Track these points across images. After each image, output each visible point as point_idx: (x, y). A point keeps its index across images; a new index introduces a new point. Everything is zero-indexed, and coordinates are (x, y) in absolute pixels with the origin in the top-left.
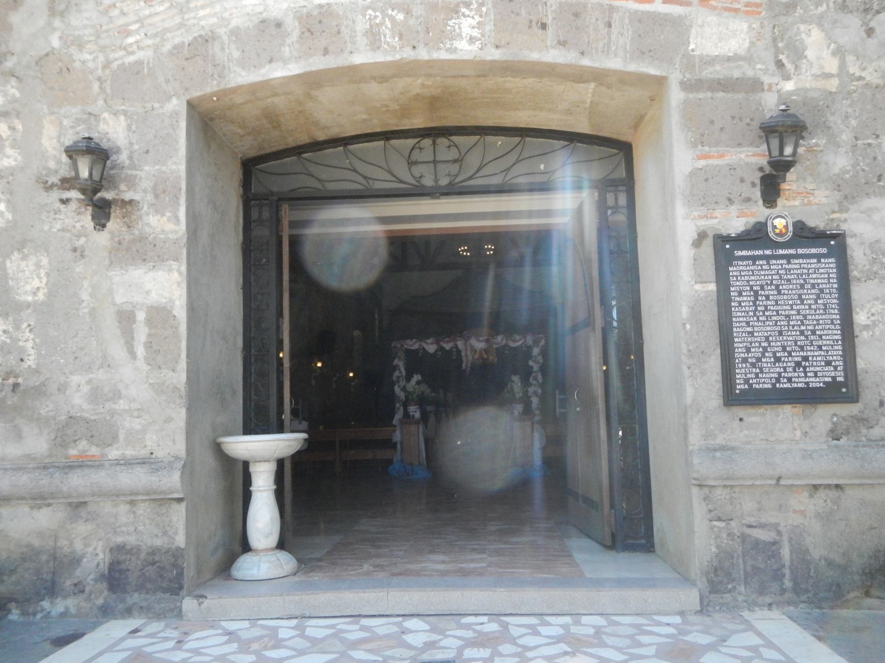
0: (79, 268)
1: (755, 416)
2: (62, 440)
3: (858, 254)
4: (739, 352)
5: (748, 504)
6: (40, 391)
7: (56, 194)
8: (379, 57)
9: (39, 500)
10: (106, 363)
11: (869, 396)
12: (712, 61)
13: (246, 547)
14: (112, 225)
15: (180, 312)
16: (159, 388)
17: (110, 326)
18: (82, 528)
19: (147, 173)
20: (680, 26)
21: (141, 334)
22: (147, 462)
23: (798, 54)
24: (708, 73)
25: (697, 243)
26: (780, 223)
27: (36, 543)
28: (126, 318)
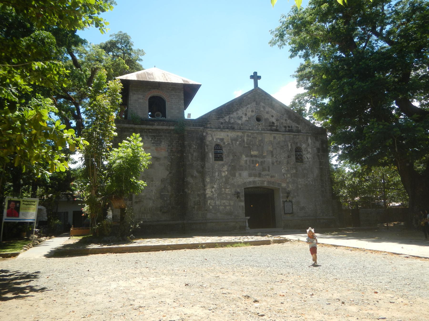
3: (293, 203)
8: (259, 185)
14: (238, 199)
15: (244, 206)
19: (241, 194)
20: (281, 184)
22: (242, 219)
23: (289, 187)
28: (240, 207)
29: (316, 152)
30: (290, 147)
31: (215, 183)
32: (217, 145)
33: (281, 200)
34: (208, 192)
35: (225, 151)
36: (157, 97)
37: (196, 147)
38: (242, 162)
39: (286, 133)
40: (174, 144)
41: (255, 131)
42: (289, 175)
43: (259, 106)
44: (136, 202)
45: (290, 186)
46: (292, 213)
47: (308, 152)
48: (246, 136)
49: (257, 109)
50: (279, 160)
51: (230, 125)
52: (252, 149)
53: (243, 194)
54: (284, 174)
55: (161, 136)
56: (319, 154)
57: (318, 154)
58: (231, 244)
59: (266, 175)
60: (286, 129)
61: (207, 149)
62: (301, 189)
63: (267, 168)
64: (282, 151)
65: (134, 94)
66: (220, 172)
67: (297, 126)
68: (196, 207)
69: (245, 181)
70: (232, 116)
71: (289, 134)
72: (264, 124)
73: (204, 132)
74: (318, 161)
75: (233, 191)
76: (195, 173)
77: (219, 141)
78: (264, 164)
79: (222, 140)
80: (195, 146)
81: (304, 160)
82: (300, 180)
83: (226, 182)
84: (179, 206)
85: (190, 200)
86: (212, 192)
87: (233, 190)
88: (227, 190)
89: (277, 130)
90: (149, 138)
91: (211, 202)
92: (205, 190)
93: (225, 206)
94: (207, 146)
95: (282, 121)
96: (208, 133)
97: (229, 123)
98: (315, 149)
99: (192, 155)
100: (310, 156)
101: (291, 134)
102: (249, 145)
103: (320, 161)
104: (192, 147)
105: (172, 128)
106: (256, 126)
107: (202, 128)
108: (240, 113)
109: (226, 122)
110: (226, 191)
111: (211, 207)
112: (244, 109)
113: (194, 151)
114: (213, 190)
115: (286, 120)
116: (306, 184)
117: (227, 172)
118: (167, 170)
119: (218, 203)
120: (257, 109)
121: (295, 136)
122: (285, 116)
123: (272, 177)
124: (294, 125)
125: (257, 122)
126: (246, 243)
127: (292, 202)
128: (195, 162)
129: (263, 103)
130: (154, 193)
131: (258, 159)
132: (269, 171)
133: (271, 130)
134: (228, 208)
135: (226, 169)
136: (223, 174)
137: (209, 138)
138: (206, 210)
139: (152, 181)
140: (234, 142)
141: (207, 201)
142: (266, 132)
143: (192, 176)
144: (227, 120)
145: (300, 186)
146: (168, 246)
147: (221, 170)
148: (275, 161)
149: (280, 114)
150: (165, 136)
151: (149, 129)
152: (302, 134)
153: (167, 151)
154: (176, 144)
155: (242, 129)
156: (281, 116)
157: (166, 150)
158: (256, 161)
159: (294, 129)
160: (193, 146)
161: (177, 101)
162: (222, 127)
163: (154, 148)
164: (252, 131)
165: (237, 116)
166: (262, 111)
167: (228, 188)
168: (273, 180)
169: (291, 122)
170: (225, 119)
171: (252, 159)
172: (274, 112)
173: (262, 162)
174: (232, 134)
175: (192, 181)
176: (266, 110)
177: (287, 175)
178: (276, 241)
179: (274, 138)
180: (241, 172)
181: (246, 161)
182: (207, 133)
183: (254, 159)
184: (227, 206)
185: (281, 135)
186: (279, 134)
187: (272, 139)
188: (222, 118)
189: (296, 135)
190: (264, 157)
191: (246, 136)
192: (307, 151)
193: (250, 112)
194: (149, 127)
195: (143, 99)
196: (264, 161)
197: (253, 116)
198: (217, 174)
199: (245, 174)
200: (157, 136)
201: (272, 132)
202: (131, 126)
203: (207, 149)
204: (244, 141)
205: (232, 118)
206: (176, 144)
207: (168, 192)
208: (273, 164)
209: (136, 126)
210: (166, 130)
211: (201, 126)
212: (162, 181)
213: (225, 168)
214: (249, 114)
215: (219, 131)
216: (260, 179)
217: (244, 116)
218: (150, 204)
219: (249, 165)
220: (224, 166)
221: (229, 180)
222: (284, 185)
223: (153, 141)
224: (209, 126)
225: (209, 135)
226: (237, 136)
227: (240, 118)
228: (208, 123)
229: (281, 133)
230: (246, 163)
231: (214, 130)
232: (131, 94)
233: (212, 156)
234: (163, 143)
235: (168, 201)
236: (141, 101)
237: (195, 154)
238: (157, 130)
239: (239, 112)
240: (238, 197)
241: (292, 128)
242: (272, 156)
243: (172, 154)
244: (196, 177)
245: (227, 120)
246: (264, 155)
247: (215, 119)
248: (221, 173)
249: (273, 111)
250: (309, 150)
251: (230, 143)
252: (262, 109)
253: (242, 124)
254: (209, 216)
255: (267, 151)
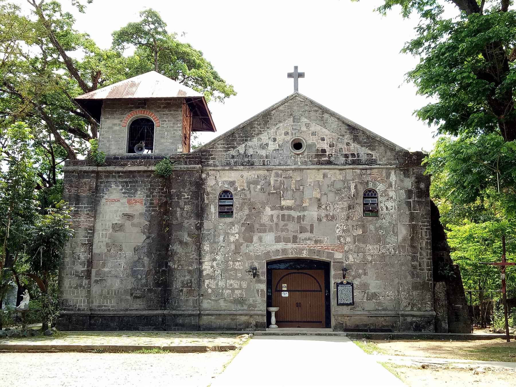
0: (251, 283)
1: (341, 307)
2: (249, 307)
3: (355, 286)
4: (339, 299)
5: (340, 318)
6: (246, 300)
7: (248, 273)
9: (246, 315)
10: (255, 297)
11: (355, 304)
12: (337, 259)
13: (271, 324)
16: (262, 301)
17: (255, 292)
18: (252, 319)
19: (260, 271)
20: (333, 254)
21: (260, 293)
24: (338, 260)
25: (334, 284)
26: (345, 282)
27: (245, 321)
28: (258, 291)
29: (405, 197)
30: (353, 191)
31: (219, 253)
32: (226, 192)
33: (332, 281)
34: (206, 267)
35: (236, 202)
36: (142, 120)
37: (189, 197)
38: (265, 219)
39: (347, 167)
40: (155, 194)
41: (288, 167)
42: (348, 239)
43: (299, 124)
44: (97, 282)
45: (350, 257)
46: (353, 304)
47: (390, 198)
48: (273, 175)
49: (296, 129)
50: (331, 214)
51: (246, 160)
52: (283, 197)
53: (265, 270)
54: (339, 238)
55: (137, 182)
56: (411, 200)
57: (409, 200)
58: (149, 349)
59: (306, 239)
60: (346, 160)
61: (208, 199)
62: (371, 262)
63: (308, 228)
64: (337, 198)
65: (108, 118)
66: (227, 234)
67: (371, 153)
68: (185, 289)
69: (269, 249)
70: (249, 143)
71: (353, 169)
72: (306, 153)
73: (202, 172)
74: (408, 212)
75: (247, 265)
76: (186, 238)
77: (227, 186)
78: (303, 221)
79: (232, 183)
80: (187, 195)
81: (380, 212)
82: (371, 247)
83: (237, 251)
84: (160, 289)
85: (175, 279)
86: (212, 267)
87: (247, 264)
88: (237, 264)
89: (329, 163)
90: (118, 186)
91: (209, 283)
92: (201, 263)
93: (233, 290)
94: (208, 194)
95: (340, 146)
96: (210, 174)
97: (246, 155)
98: (402, 192)
99: (182, 209)
100: (393, 205)
101: (356, 169)
102: (278, 190)
103: (411, 214)
104: (183, 198)
105: (153, 168)
106: (292, 158)
107: (198, 166)
108: (264, 138)
109: (240, 154)
110: (235, 265)
111: (210, 291)
112: (273, 130)
113: (186, 203)
114: (215, 264)
115: (348, 144)
116: (383, 253)
117: (237, 235)
118: (144, 233)
119: (221, 284)
120: (296, 129)
121: (364, 171)
122: (346, 137)
123: (316, 242)
124: (363, 152)
125: (293, 151)
126: (166, 349)
127: (352, 286)
128: (186, 221)
129: (306, 117)
130: (122, 268)
131: (292, 213)
132: (312, 232)
133: (320, 163)
134: (236, 292)
135: (237, 231)
136: (232, 239)
137: (210, 182)
138: (202, 295)
139: (121, 250)
140: (252, 186)
141: (204, 281)
142: (308, 167)
143: (181, 242)
144: (242, 151)
145: (370, 258)
146: (52, 347)
147: (229, 231)
148: (323, 215)
149: (337, 134)
150: (142, 181)
151: (119, 172)
152: (378, 166)
153: (145, 204)
154: (159, 192)
155: (268, 165)
156: (339, 138)
157: (144, 203)
158: (289, 216)
159: (364, 158)
160: (184, 196)
161: (172, 125)
162: (232, 163)
163: (125, 200)
164: (285, 167)
165: (259, 143)
166: (304, 132)
167: (239, 261)
168: (318, 247)
169: (358, 146)
170: (238, 151)
171: (282, 212)
172: (326, 131)
173: (299, 218)
174: (250, 174)
175: (181, 249)
176: (310, 129)
177: (345, 239)
178: (217, 349)
179: (325, 176)
180: (261, 234)
181: (272, 216)
182: (208, 174)
183: (286, 212)
184: (237, 289)
185: (337, 172)
186: (334, 169)
187: (320, 177)
188: (234, 148)
189: (366, 169)
190: (304, 209)
191: (273, 175)
192: (387, 195)
193: (283, 135)
194: (118, 169)
195: (119, 125)
196: (304, 216)
197: (287, 142)
198: (221, 238)
199: (269, 237)
200: (130, 181)
201: (319, 167)
202: (92, 168)
203: (208, 199)
204: (270, 184)
205: (250, 147)
206: (159, 192)
207: (144, 266)
208: (320, 220)
209: (100, 169)
210: (145, 172)
211: (198, 164)
212: (135, 250)
213: (236, 229)
214: (281, 138)
215: (228, 170)
216: (294, 246)
217: (271, 143)
218: (116, 284)
219: (277, 224)
220: (234, 226)
221: (241, 247)
222: (338, 256)
223: (124, 190)
224: (211, 162)
225: (212, 177)
226: (258, 177)
227: (264, 146)
228: (210, 157)
229: (337, 167)
230: (272, 220)
231: (219, 168)
232: (102, 119)
233: (215, 210)
234: (139, 192)
235: (144, 281)
236: (117, 128)
237: (187, 208)
238: (131, 172)
239: (261, 136)
240: (255, 275)
241: (358, 157)
242: (319, 207)
243: (151, 209)
244: (186, 244)
245: (242, 151)
246: (304, 205)
247: (221, 151)
248: (228, 237)
249: (324, 130)
250: (392, 194)
251: (246, 188)
252: (304, 129)
253: (267, 157)
254: (206, 304)
255: (310, 199)
